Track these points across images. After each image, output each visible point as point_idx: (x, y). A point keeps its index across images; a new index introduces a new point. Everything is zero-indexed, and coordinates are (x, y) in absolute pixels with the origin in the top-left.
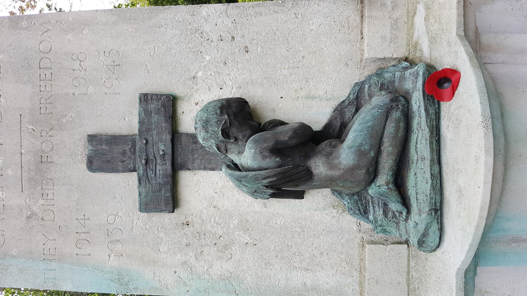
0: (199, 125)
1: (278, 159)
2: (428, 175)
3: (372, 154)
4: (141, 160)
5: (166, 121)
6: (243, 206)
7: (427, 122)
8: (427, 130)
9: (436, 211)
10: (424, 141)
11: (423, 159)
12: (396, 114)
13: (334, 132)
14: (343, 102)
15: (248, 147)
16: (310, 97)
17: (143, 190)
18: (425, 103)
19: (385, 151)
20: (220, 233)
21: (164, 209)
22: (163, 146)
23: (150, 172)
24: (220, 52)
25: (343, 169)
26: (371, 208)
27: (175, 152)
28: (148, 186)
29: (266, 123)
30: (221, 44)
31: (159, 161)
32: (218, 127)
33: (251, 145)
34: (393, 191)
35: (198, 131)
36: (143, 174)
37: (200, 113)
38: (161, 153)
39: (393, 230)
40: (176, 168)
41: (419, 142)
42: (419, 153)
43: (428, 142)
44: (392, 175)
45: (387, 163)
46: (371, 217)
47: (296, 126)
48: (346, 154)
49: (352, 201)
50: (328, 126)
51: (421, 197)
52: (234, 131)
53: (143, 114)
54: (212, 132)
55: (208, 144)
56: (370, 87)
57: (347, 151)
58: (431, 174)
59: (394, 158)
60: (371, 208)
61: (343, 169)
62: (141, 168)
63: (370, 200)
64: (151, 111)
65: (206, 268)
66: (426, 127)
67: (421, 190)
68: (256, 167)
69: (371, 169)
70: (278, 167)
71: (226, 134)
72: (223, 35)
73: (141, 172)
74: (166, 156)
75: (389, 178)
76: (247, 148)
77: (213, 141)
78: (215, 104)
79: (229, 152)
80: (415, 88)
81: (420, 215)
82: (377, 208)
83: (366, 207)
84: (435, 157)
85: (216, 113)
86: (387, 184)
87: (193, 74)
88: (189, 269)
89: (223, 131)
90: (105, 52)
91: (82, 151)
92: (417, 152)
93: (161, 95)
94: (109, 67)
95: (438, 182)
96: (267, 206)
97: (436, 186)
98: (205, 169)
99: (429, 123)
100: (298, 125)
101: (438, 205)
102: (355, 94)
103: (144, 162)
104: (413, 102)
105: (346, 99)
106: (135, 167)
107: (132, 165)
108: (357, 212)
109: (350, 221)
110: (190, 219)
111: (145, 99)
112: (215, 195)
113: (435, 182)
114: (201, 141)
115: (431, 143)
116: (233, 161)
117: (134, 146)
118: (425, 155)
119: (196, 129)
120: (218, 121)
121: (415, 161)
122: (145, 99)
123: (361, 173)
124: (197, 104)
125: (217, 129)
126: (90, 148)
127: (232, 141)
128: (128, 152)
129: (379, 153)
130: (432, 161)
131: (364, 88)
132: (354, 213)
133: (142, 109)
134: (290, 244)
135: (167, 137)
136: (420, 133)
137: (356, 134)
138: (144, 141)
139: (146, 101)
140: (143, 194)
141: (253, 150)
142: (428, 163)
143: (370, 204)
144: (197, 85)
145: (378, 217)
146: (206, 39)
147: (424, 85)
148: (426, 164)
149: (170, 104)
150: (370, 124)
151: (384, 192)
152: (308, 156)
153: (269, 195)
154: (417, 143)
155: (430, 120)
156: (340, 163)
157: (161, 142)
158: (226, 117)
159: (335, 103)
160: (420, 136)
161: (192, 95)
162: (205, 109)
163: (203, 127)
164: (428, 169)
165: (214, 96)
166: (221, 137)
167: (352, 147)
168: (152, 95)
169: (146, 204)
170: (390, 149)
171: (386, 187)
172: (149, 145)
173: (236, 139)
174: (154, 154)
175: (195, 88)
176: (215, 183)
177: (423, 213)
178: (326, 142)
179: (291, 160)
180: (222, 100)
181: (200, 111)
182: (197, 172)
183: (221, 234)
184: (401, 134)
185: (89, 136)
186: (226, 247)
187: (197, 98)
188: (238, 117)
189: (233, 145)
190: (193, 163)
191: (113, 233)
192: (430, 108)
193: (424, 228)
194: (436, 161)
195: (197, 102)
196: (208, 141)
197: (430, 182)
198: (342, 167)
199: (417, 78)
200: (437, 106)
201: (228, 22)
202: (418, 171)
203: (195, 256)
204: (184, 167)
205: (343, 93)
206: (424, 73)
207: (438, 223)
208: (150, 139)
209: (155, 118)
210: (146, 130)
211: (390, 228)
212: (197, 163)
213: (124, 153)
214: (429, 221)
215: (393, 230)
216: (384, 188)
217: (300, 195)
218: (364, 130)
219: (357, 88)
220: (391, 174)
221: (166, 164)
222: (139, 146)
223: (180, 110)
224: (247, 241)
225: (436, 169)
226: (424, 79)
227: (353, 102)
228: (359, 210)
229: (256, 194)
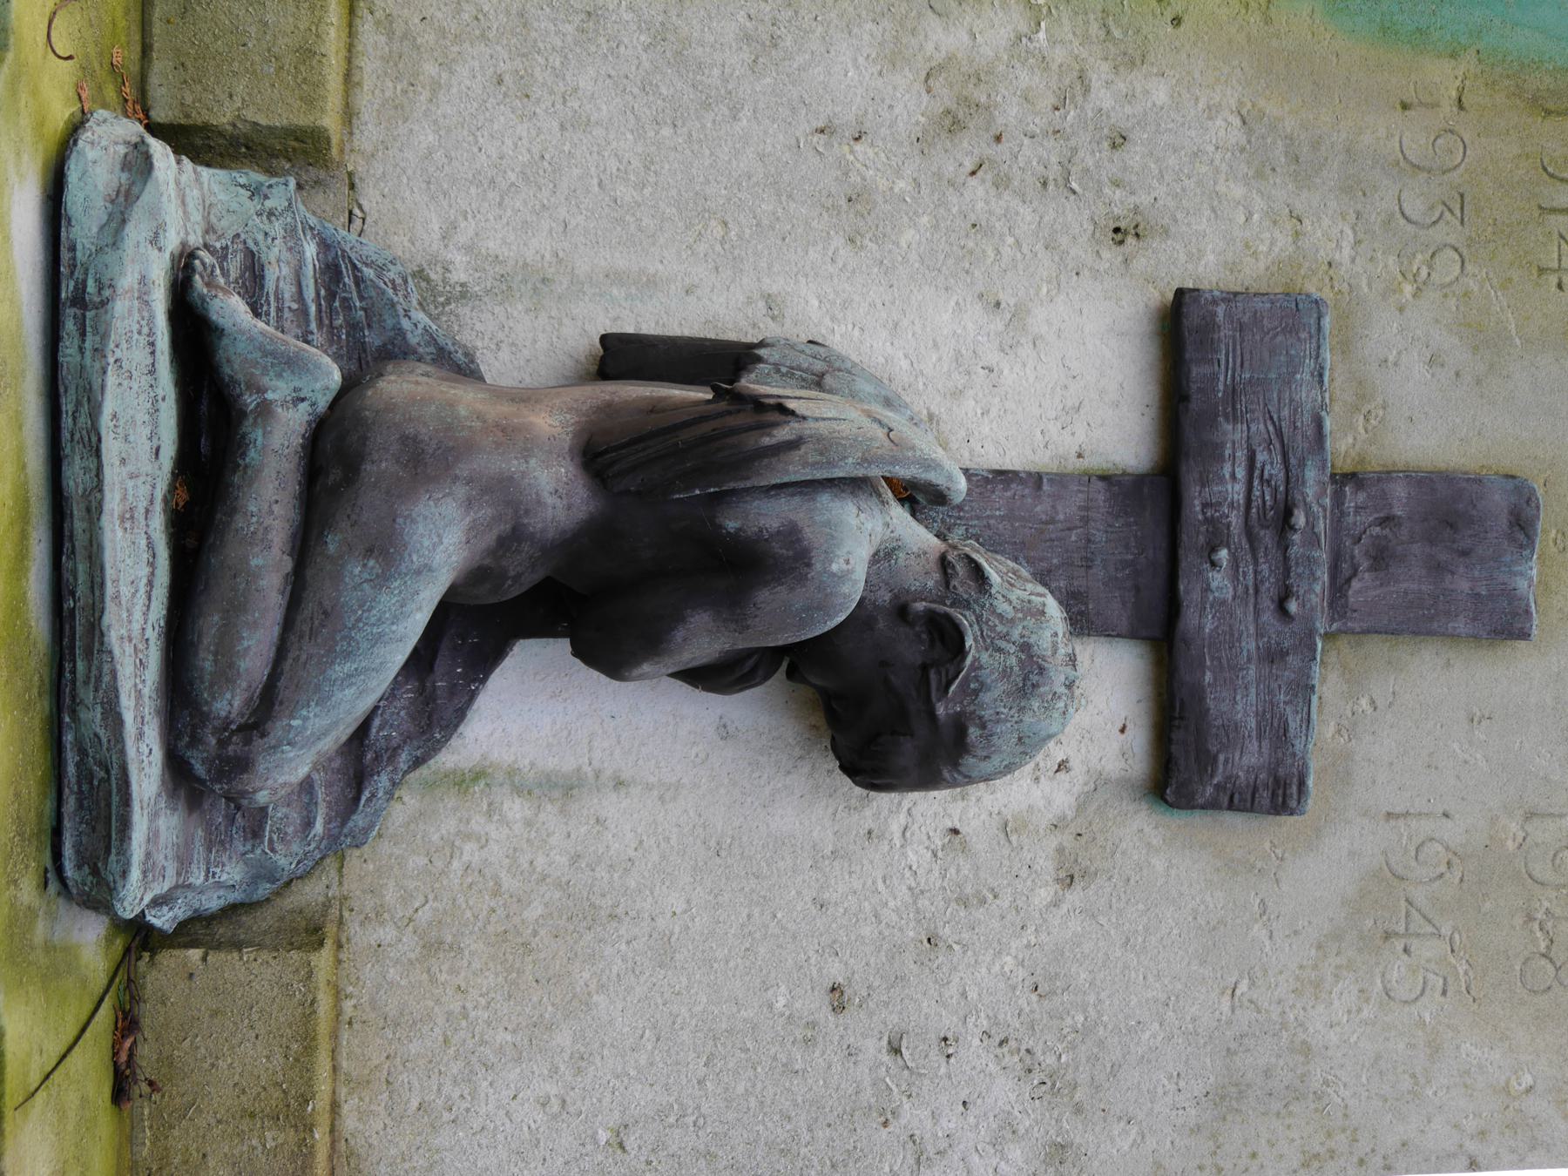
0: (1058, 678)
1: (731, 525)
2: (111, 448)
3: (333, 544)
4: (1311, 524)
5: (1198, 693)
6: (873, 305)
7: (114, 673)
8: (113, 637)
9: (79, 300)
10: (125, 591)
11: (128, 517)
13: (472, 633)
14: (418, 762)
15: (855, 582)
16: (563, 789)
17: (1306, 394)
18: (123, 752)
19: (276, 551)
20: (978, 190)
21: (1220, 310)
22: (1217, 586)
23: (1275, 470)
24: (953, 990)
25: (456, 478)
26: (310, 293)
27: (1162, 558)
28: (1285, 413)
29: (766, 678)
30: (948, 1022)
31: (1235, 520)
32: (977, 666)
33: (845, 589)
34: (240, 377)
35: (1062, 651)
36: (1302, 464)
37: (1054, 729)
38: (1223, 554)
39: (222, 196)
41: (142, 590)
42: (144, 542)
43: (110, 589)
44: (242, 445)
45: (268, 497)
46: (311, 250)
47: (646, 668)
49: (390, 322)
50: (485, 660)
51: (136, 356)
52: (910, 649)
53: (1293, 725)
54: (1002, 644)
55: (1024, 595)
56: (308, 824)
57: (438, 558)
58: (98, 453)
59: (239, 521)
60: (310, 293)
61: (456, 478)
62: (1310, 491)
63: (313, 326)
64: (1259, 738)
65: (1042, 35)
66: (117, 652)
67: (135, 386)
68: (824, 498)
69: (335, 475)
70: (733, 492)
71: (946, 639)
72: (935, 1057)
73: (1311, 474)
74: (1202, 539)
75: (258, 435)
76: (860, 573)
77: (1003, 607)
78: (987, 767)
79: (934, 556)
80: (154, 816)
81: (143, 280)
82: (288, 291)
83: (332, 295)
84: (79, 525)
85: (983, 726)
86: (265, 409)
87: (1074, 897)
88: (1117, 33)
89: (959, 650)
90: (1444, 993)
92: (150, 545)
93: (1212, 805)
94: (1430, 929)
95: (67, 422)
96: (761, 304)
97: (78, 404)
98: (1036, 480)
99: (106, 668)
100: (636, 672)
101: (70, 326)
102: (366, 794)
103: (1300, 519)
104: (158, 756)
105: (406, 773)
106: (1338, 499)
107: (1349, 504)
108: (369, 273)
110: (1106, 254)
111: (1279, 793)
112: (992, 357)
113: (83, 420)
114: (1053, 608)
115: (97, 583)
116: (913, 515)
117: (1338, 588)
118: (120, 533)
119: (1072, 660)
120: (976, 693)
121: (158, 506)
122: (1279, 793)
123: (381, 465)
124: (1062, 766)
125: (985, 657)
126: (1522, 584)
127: (920, 606)
128: (1365, 564)
129: (304, 545)
130: (94, 511)
131: (328, 822)
132: (381, 270)
133: (1299, 746)
134: (666, 131)
136: (136, 627)
137: (399, 629)
138: (1293, 607)
139: (1277, 780)
140: (1304, 375)
141: (834, 567)
142: (113, 502)
143: (313, 309)
144: (1060, 850)
145: (286, 255)
146: (1012, 1043)
147: (125, 825)
148: (118, 496)
150: (340, 670)
151: (279, 376)
153: (759, 359)
154: (150, 583)
155: (99, 679)
156: (469, 504)
157: (1223, 602)
158: (941, 710)
160: (138, 615)
161: (1081, 807)
162: (1028, 745)
163: (1042, 670)
164: (113, 473)
165: (987, 799)
166: (965, 620)
167: (418, 572)
168: (1251, 810)
169: (1292, 330)
170: (255, 562)
171: (270, 396)
172: (1274, 592)
173: (901, 611)
174: (1253, 550)
175: (1067, 839)
176: (994, 412)
177: (131, 290)
178: (515, 592)
179: (674, 526)
180: (953, 784)
181: (1050, 737)
182: (1074, 465)
183: (973, 181)
184: (209, 625)
185: (1524, 635)
187: (1059, 796)
188: (888, 707)
189: (915, 586)
190: (1087, 509)
191: (1441, 207)
192: (101, 732)
193: (130, 228)
194: (77, 511)
195: (1062, 775)
197: (105, 420)
198: (461, 491)
199: (148, 855)
200: (69, 738)
202: (147, 467)
203: (1087, 90)
206: (125, 874)
207: (73, 249)
208: (1268, 617)
210: (1283, 654)
211: (234, 206)
212: (1068, 509)
213: (1381, 558)
214: (110, 257)
215: (222, 196)
216: (278, 389)
217: (621, 356)
218: (364, 645)
219: (359, 820)
220: (252, 453)
221: (1205, 505)
222: (1318, 588)
223: (1139, 739)
224: (858, 147)
225: (75, 475)
226: (124, 853)
227: (377, 758)
228: (358, 281)
229: (819, 366)
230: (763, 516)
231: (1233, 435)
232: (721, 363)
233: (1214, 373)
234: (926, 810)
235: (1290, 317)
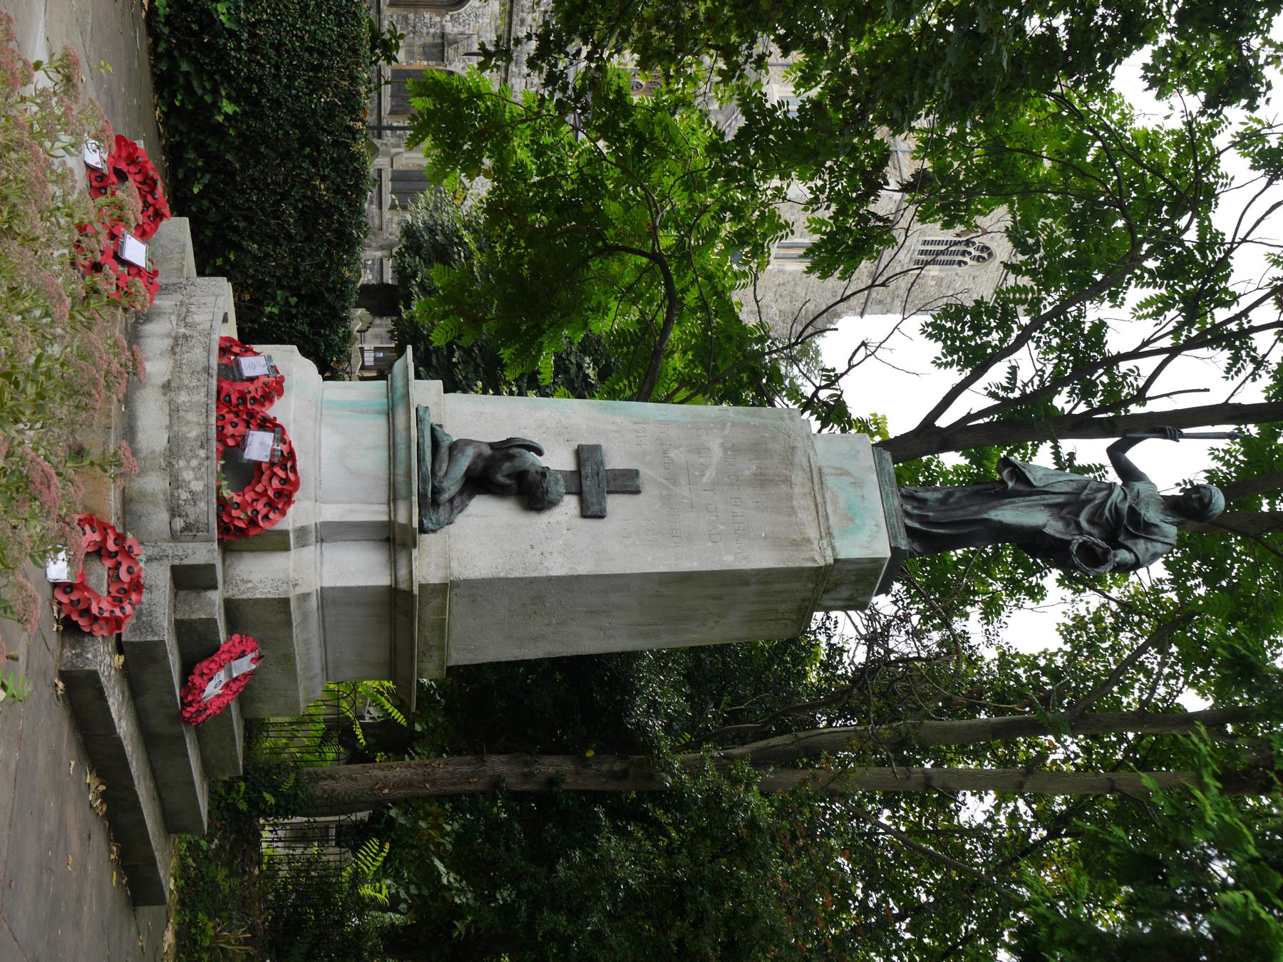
12: (441, 474)
22: (587, 484)
40: (578, 473)
45: (444, 451)
52: (539, 477)
91: (643, 482)
135: (585, 488)
149: (585, 514)
152: (492, 457)
159: (465, 512)
186: (540, 427)
187: (567, 517)
201: (545, 564)
209: (594, 500)
231: (588, 464)
233: (584, 455)
235: (597, 448)
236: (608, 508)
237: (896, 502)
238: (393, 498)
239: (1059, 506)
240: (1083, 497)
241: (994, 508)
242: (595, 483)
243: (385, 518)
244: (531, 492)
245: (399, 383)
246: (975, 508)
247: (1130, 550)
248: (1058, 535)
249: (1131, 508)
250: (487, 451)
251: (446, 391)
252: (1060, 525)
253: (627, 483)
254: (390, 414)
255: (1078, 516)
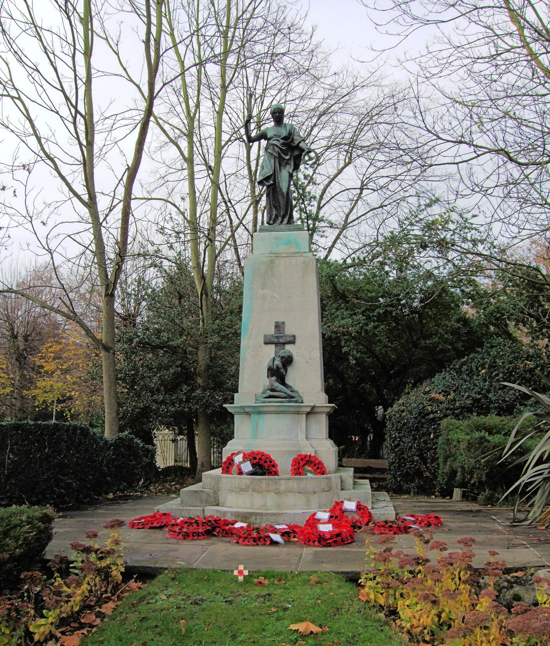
22: (281, 341)
40: (276, 344)
48: (277, 385)
71: (283, 357)
91: (280, 320)
109: (261, 390)
111: (294, 336)
122: (294, 336)
149: (293, 342)
162: (289, 352)
196: (282, 353)
204: (276, 347)
205: (296, 388)
230: (275, 367)
232: (268, 370)
234: (295, 358)
235: (265, 336)
236: (291, 334)
237: (283, 226)
238: (298, 413)
239: (280, 165)
240: (277, 156)
241: (281, 190)
242: (280, 339)
243: (305, 415)
244: (288, 361)
245: (238, 410)
246: (280, 197)
247: (300, 142)
248: (292, 167)
249: (282, 139)
250: (274, 378)
251: (237, 392)
252: (288, 166)
253: (279, 326)
254: (260, 413)
255: (285, 159)
